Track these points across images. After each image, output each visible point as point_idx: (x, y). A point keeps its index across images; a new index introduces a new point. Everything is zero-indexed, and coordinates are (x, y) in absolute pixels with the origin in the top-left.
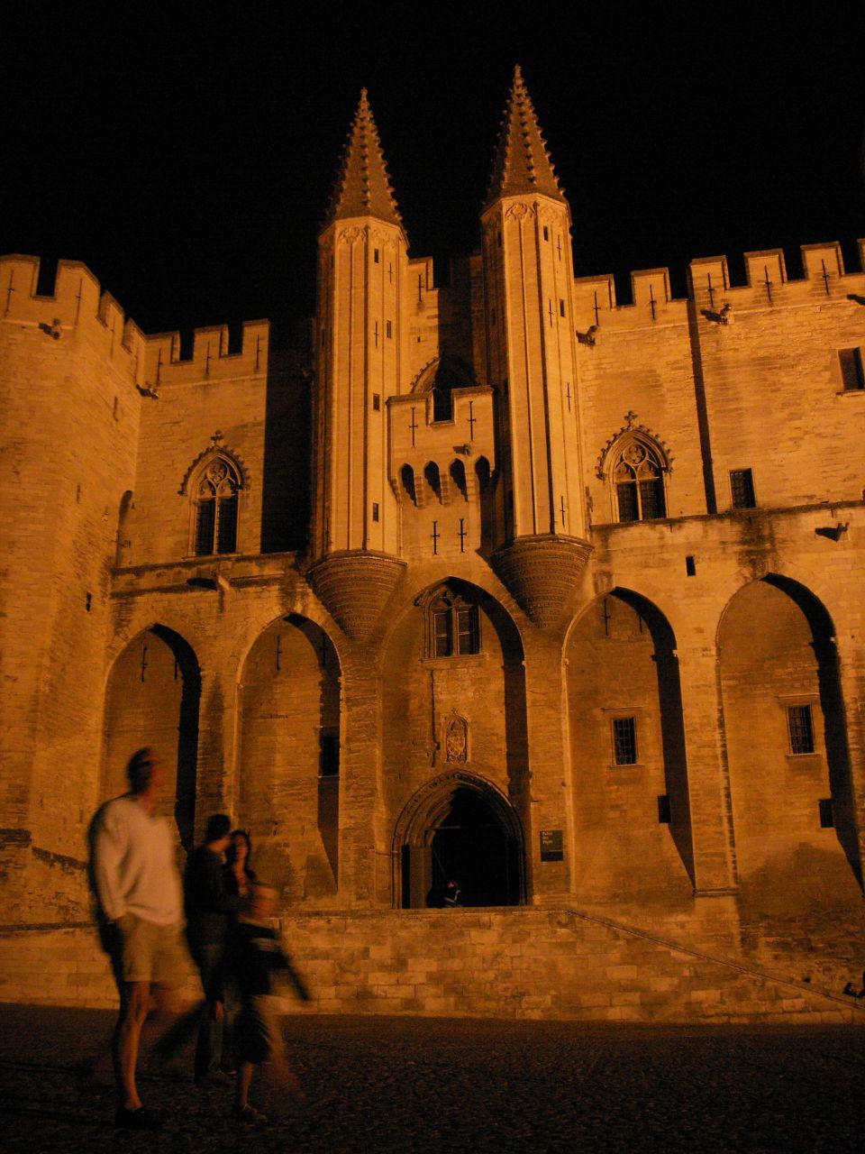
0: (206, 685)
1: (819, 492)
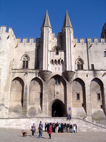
0: (25, 85)
1: (102, 68)
